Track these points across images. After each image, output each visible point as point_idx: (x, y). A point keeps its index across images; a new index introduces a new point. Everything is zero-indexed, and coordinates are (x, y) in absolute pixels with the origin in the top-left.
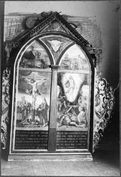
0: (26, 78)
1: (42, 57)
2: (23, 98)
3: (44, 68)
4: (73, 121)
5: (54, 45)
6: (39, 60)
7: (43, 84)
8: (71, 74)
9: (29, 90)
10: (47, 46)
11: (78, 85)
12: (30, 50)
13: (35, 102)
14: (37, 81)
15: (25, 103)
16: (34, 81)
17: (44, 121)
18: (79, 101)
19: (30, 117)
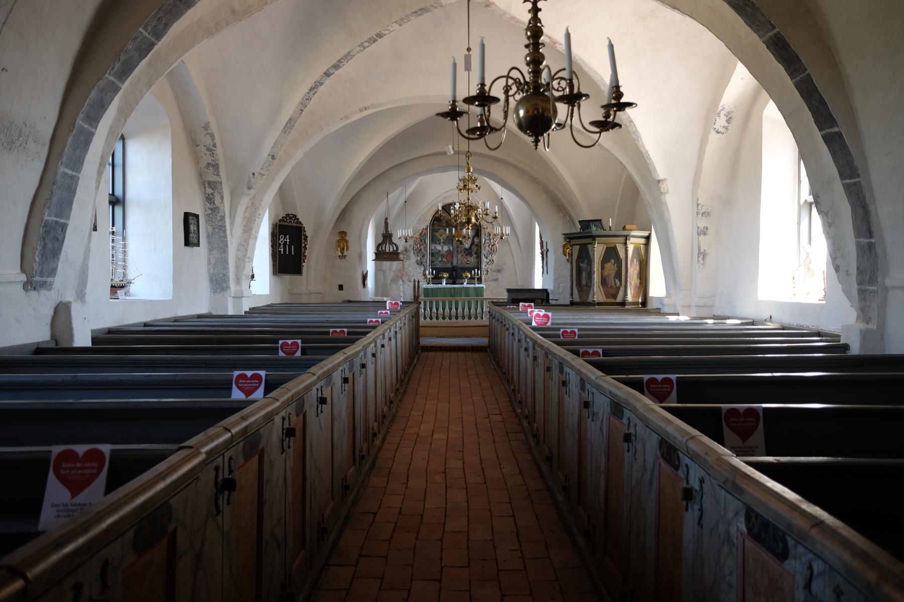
0: (436, 234)
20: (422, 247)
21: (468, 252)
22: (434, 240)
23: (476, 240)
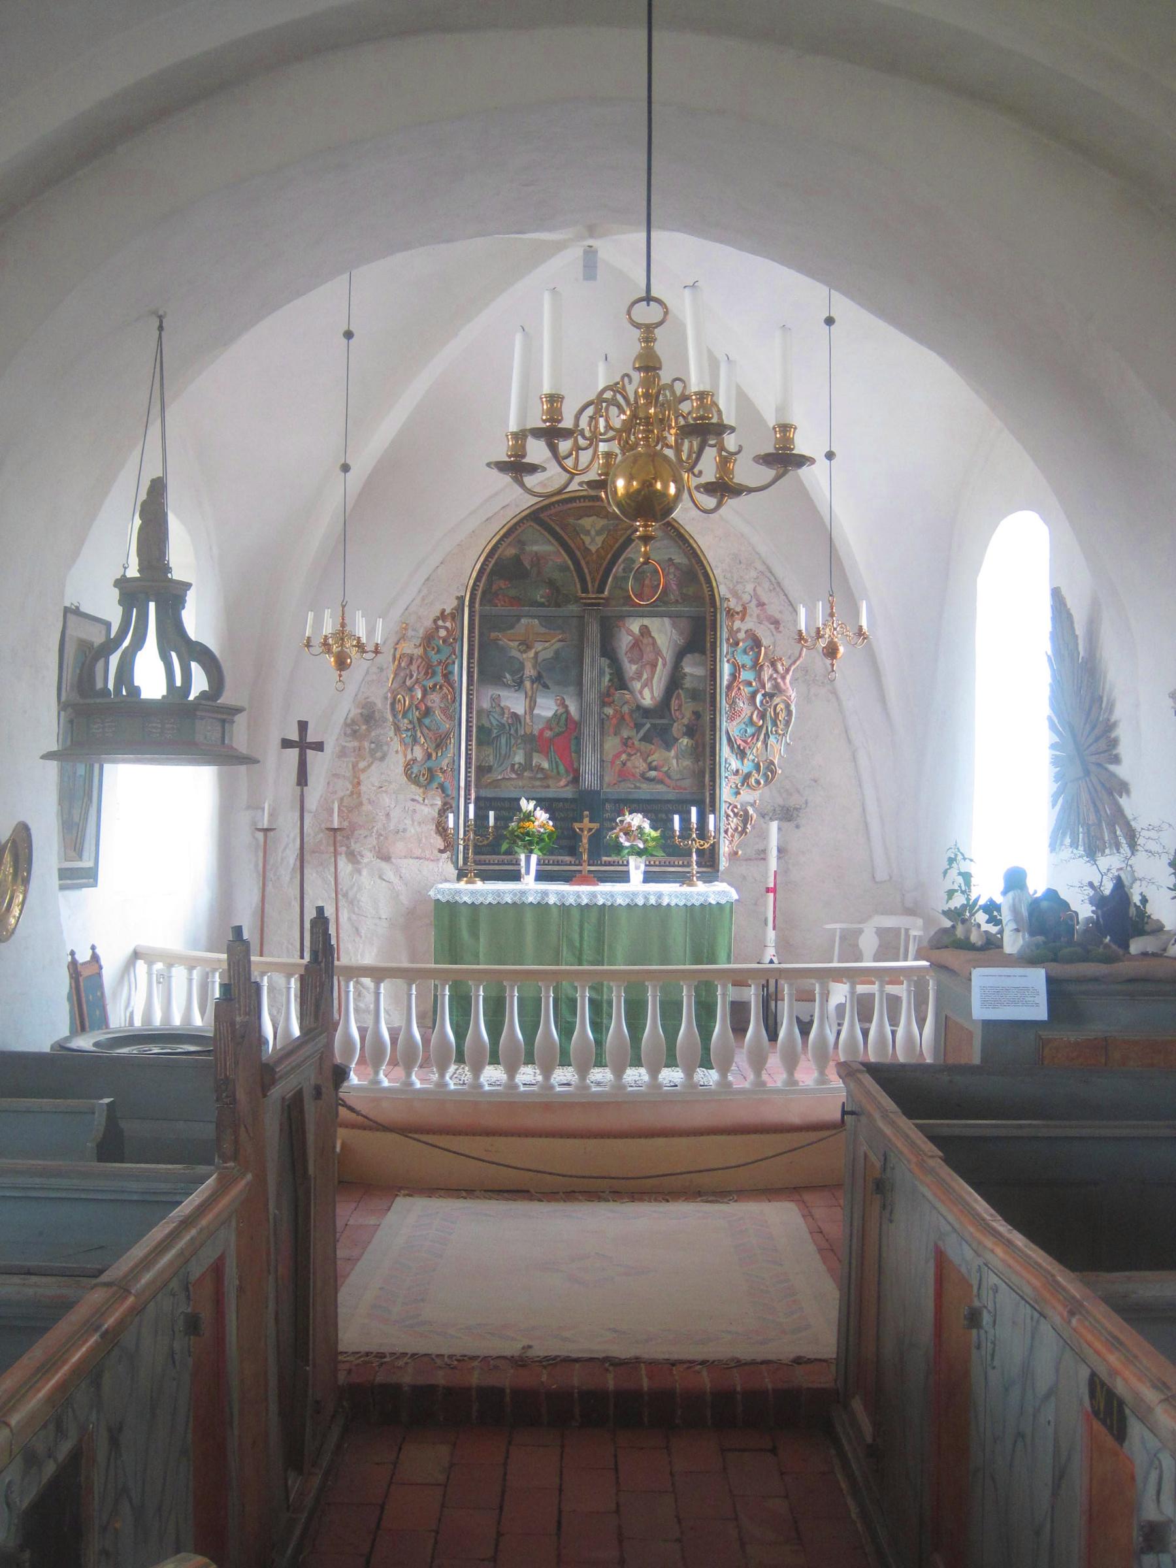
2: (496, 700)
3: (558, 605)
4: (655, 769)
5: (588, 533)
7: (557, 652)
8: (646, 621)
9: (513, 673)
12: (511, 551)
13: (532, 709)
14: (539, 646)
15: (503, 714)
16: (527, 646)
17: (562, 768)
18: (674, 704)
19: (519, 758)
20: (435, 699)
21: (655, 724)
22: (491, 668)
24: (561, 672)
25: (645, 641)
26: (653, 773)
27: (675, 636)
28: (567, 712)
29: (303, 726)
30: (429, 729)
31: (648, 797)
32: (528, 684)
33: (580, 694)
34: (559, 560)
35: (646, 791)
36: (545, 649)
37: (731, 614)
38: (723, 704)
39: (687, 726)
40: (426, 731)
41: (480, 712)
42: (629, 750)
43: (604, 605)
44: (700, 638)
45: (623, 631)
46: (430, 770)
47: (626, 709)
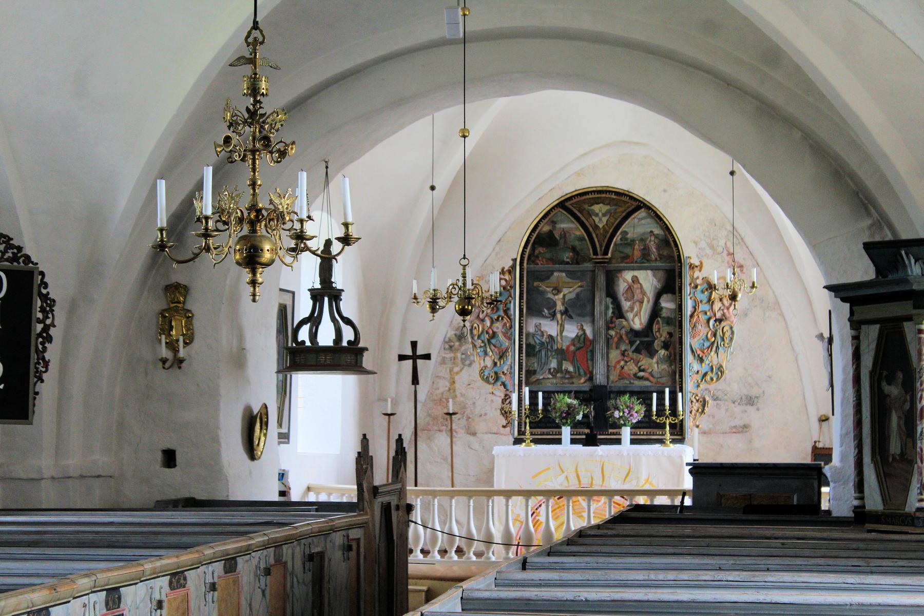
0: (543, 286)
1: (572, 241)
2: (538, 327)
3: (578, 263)
4: (643, 371)
5: (597, 215)
6: (568, 247)
7: (578, 295)
8: (636, 273)
9: (549, 309)
10: (583, 219)
11: (650, 294)
12: (546, 228)
14: (565, 291)
15: (543, 335)
16: (557, 290)
17: (582, 371)
18: (655, 327)
19: (554, 364)
21: (643, 341)
22: (535, 305)
23: (667, 304)
24: (578, 308)
25: (635, 286)
26: (641, 374)
27: (655, 282)
28: (585, 333)
29: (414, 344)
30: (495, 346)
31: (639, 389)
32: (559, 316)
33: (593, 322)
34: (578, 233)
35: (638, 384)
36: (570, 291)
37: (692, 267)
38: (687, 326)
39: (664, 342)
40: (493, 347)
41: (528, 335)
42: (626, 359)
43: (608, 263)
44: (672, 283)
45: (621, 280)
46: (496, 373)
47: (623, 332)
